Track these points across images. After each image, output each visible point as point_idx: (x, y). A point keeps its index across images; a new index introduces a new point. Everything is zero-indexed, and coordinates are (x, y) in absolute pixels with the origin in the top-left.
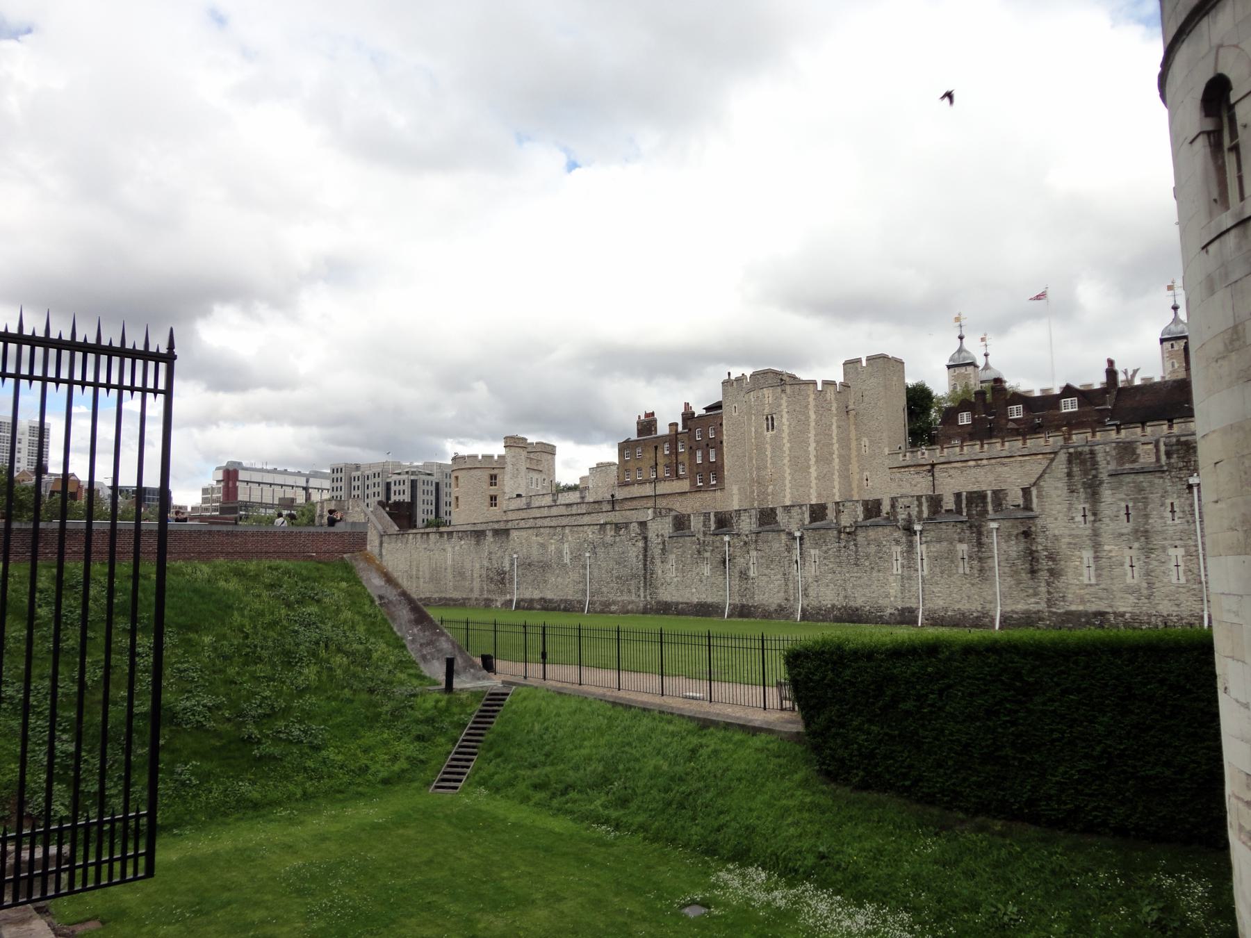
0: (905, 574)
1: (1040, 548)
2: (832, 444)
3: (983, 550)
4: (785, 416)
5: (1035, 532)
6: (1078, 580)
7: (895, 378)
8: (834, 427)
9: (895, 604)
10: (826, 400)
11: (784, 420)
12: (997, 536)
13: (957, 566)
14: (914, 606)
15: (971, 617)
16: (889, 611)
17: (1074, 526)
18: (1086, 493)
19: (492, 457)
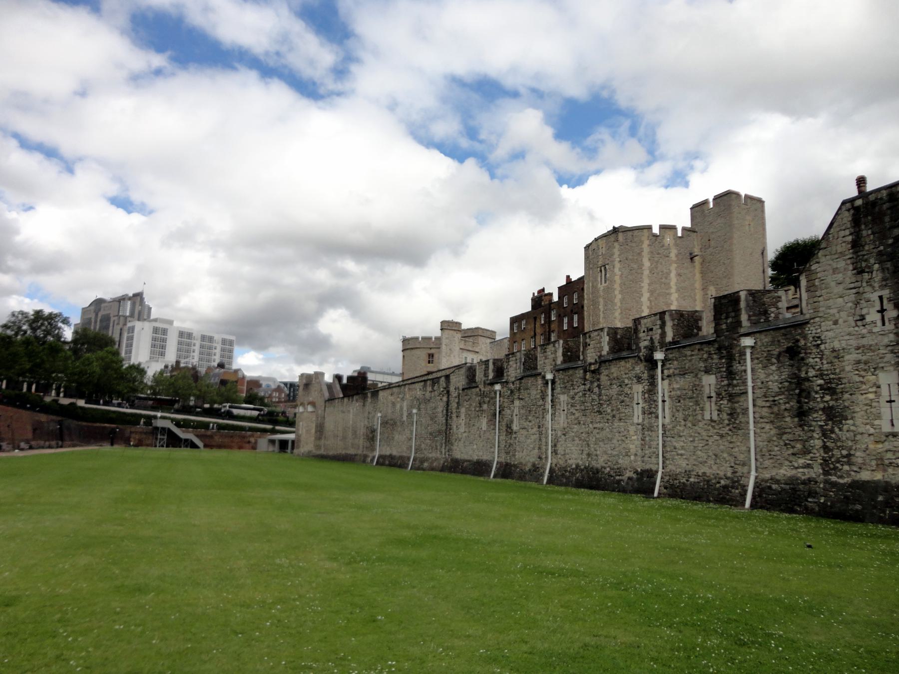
0: (646, 422)
1: (812, 373)
2: (670, 294)
3: (735, 382)
4: (617, 265)
5: (805, 348)
6: (872, 426)
7: (749, 218)
8: (673, 275)
9: (634, 464)
10: (663, 246)
11: (617, 270)
12: (752, 359)
13: (702, 409)
14: (654, 468)
15: (718, 485)
16: (629, 474)
17: (864, 331)
18: (883, 270)
19: (430, 338)
